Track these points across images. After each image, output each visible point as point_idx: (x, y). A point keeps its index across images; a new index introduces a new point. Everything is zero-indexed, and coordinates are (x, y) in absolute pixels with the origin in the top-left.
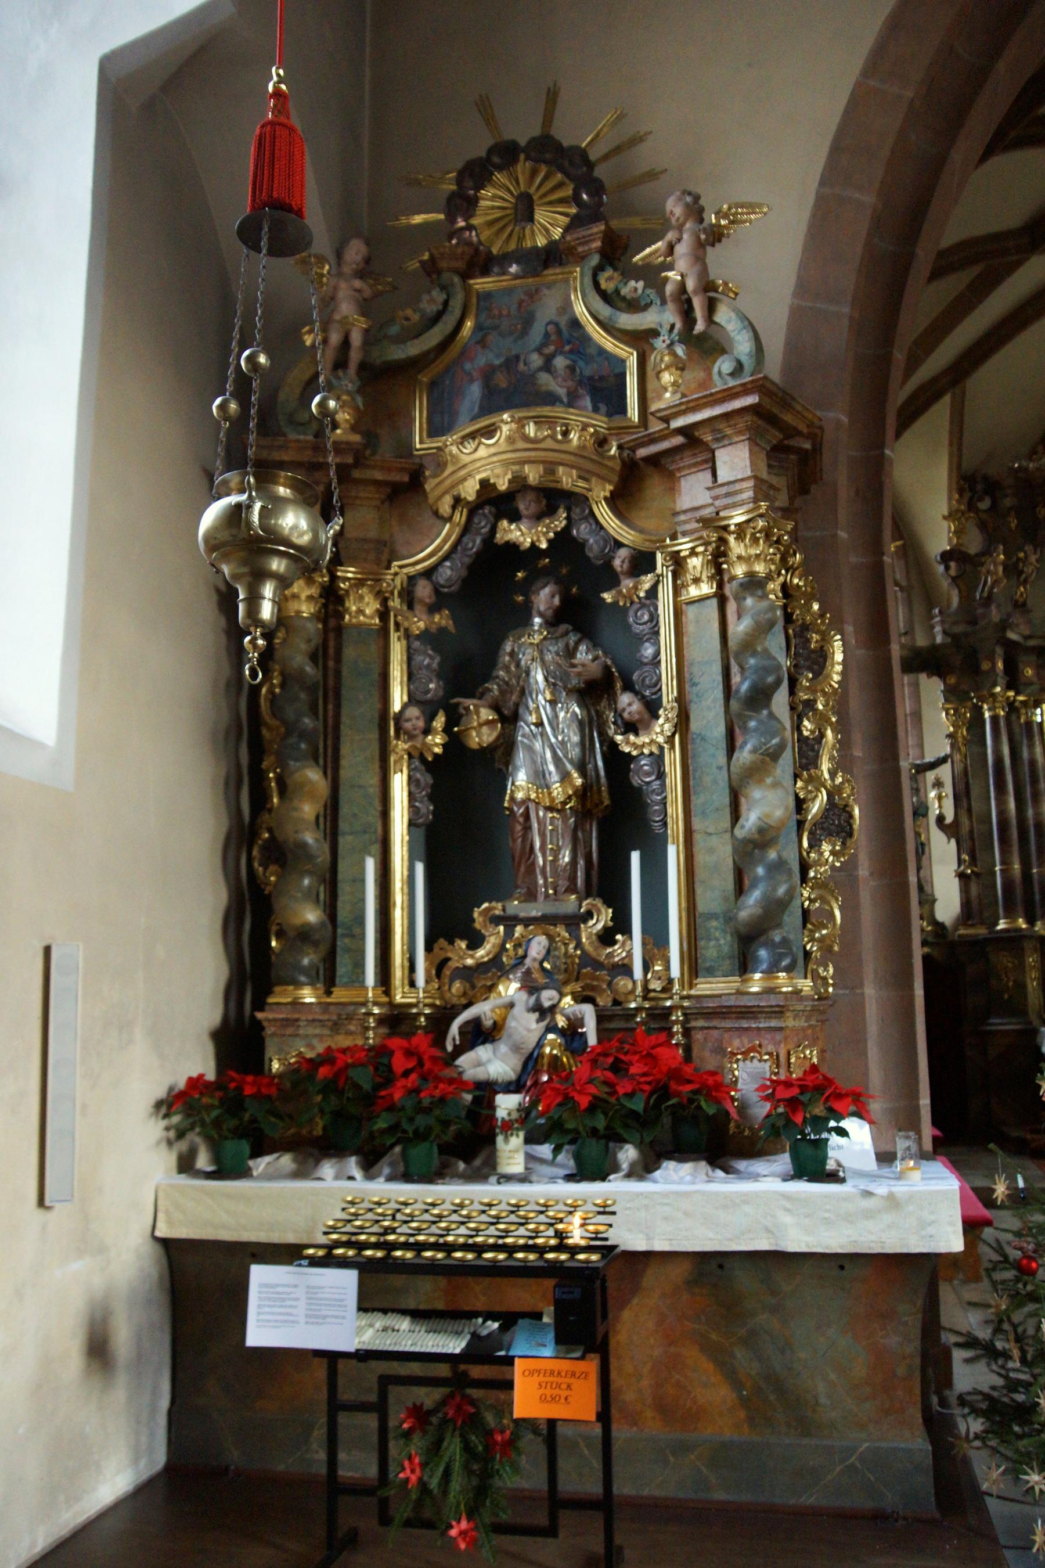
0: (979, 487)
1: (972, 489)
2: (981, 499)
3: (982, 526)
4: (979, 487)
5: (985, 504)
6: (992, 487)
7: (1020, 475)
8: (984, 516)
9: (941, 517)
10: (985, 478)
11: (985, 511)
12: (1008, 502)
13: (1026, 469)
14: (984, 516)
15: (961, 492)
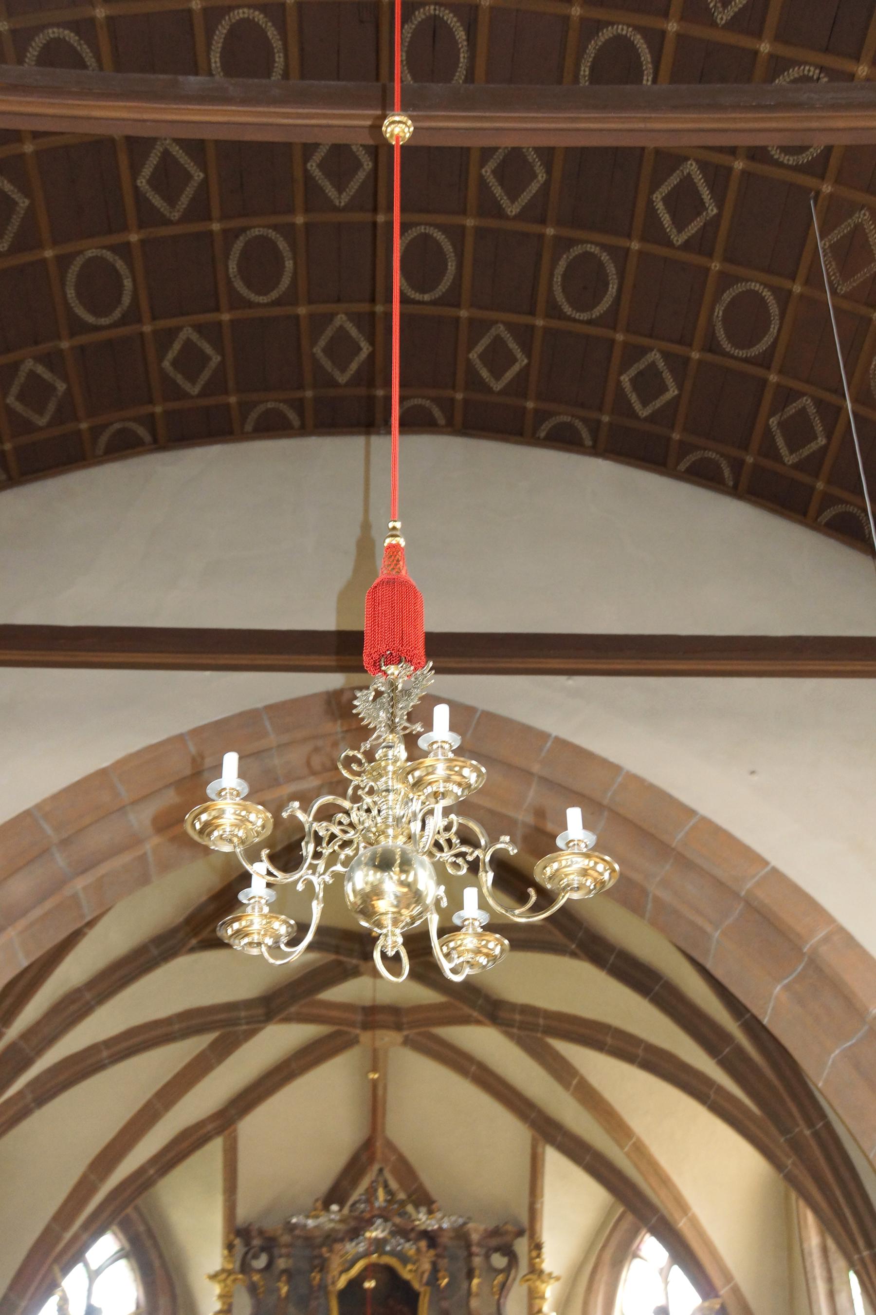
0: (256, 1242)
1: (247, 1243)
2: (256, 1257)
3: (253, 1289)
4: (256, 1242)
5: (261, 1262)
6: (270, 1245)
7: (297, 1232)
8: (256, 1278)
9: (205, 1277)
10: (261, 1232)
11: (261, 1271)
12: (282, 1263)
13: (305, 1226)
14: (256, 1278)
15: (230, 1247)
